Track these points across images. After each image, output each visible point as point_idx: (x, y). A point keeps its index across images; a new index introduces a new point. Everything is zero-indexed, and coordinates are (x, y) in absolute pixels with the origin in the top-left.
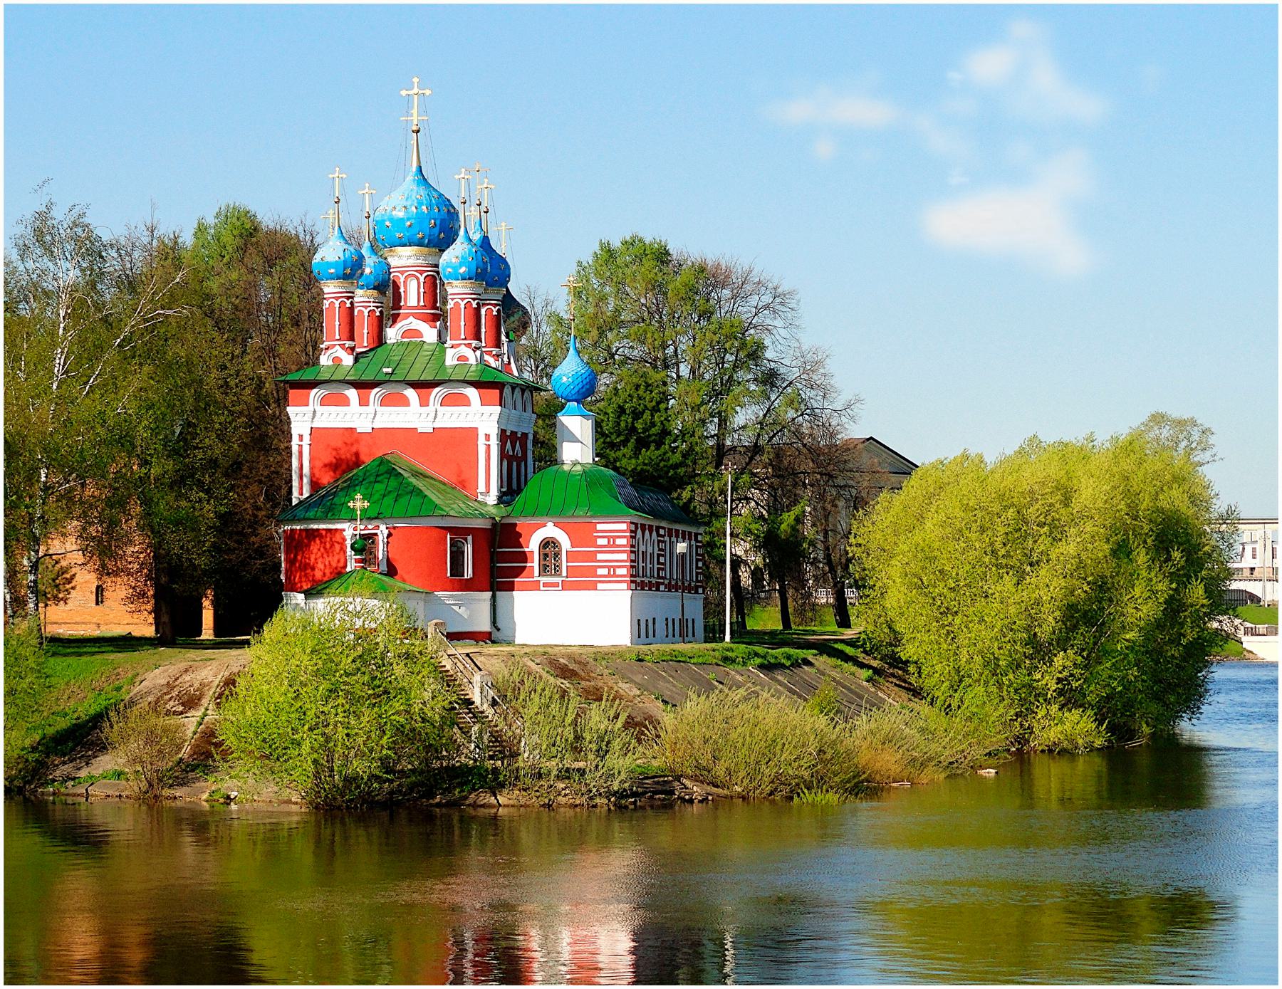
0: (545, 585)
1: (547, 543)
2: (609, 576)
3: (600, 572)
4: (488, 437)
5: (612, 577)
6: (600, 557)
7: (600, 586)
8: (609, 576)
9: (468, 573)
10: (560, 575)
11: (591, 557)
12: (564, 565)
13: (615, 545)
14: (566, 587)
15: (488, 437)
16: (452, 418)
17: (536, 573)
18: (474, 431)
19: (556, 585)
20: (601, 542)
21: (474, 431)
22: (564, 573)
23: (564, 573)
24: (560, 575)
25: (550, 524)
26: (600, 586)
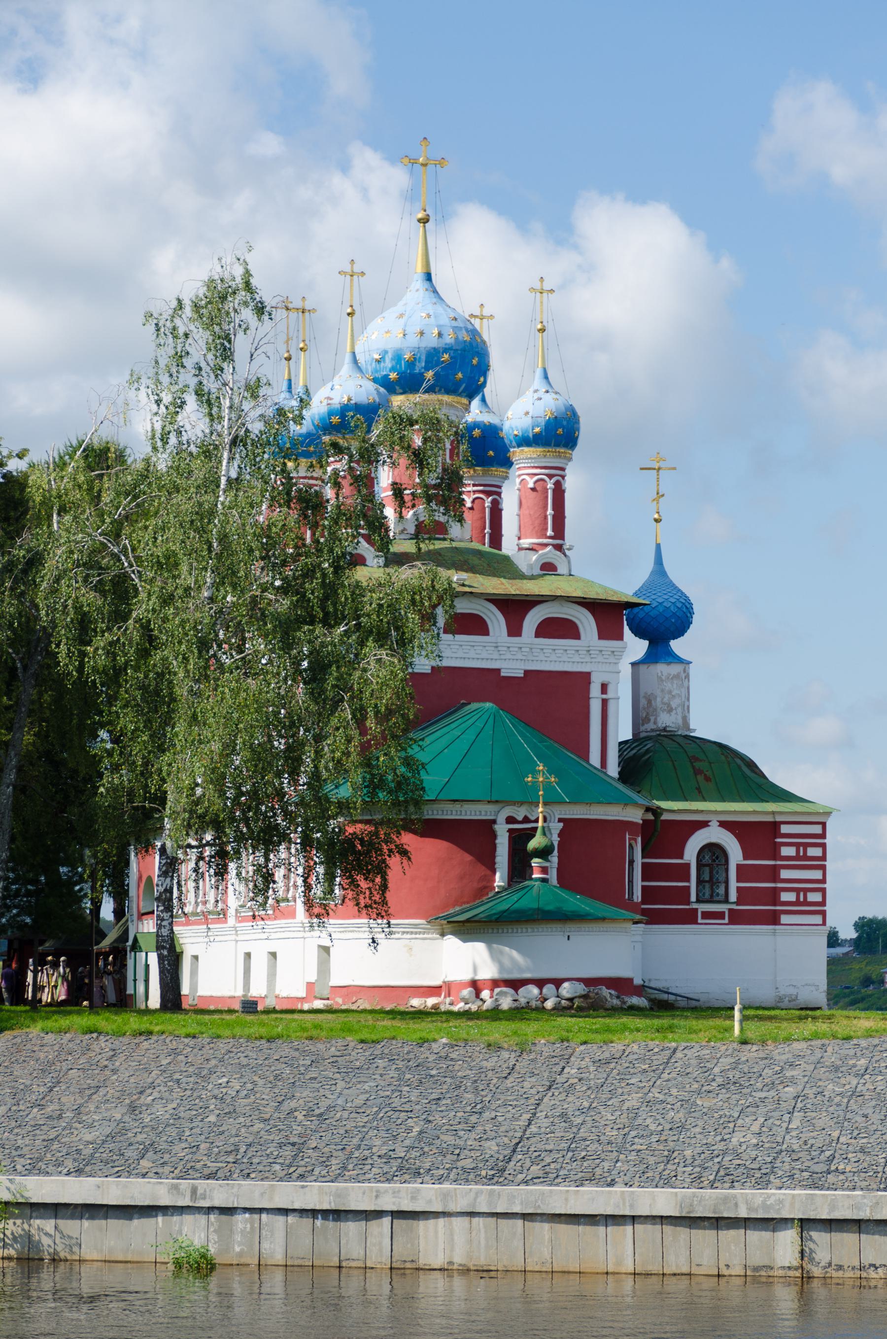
0: (707, 915)
1: (713, 854)
2: (797, 903)
3: (786, 897)
4: (604, 688)
5: (802, 906)
6: (785, 874)
7: (784, 919)
8: (797, 903)
9: (638, 896)
10: (726, 901)
11: (773, 874)
12: (733, 884)
13: (806, 857)
14: (736, 918)
15: (604, 688)
16: (556, 657)
17: (693, 898)
18: (585, 677)
19: (720, 915)
20: (787, 851)
21: (585, 677)
22: (733, 896)
23: (733, 896)
24: (726, 901)
25: (714, 824)
26: (784, 919)
